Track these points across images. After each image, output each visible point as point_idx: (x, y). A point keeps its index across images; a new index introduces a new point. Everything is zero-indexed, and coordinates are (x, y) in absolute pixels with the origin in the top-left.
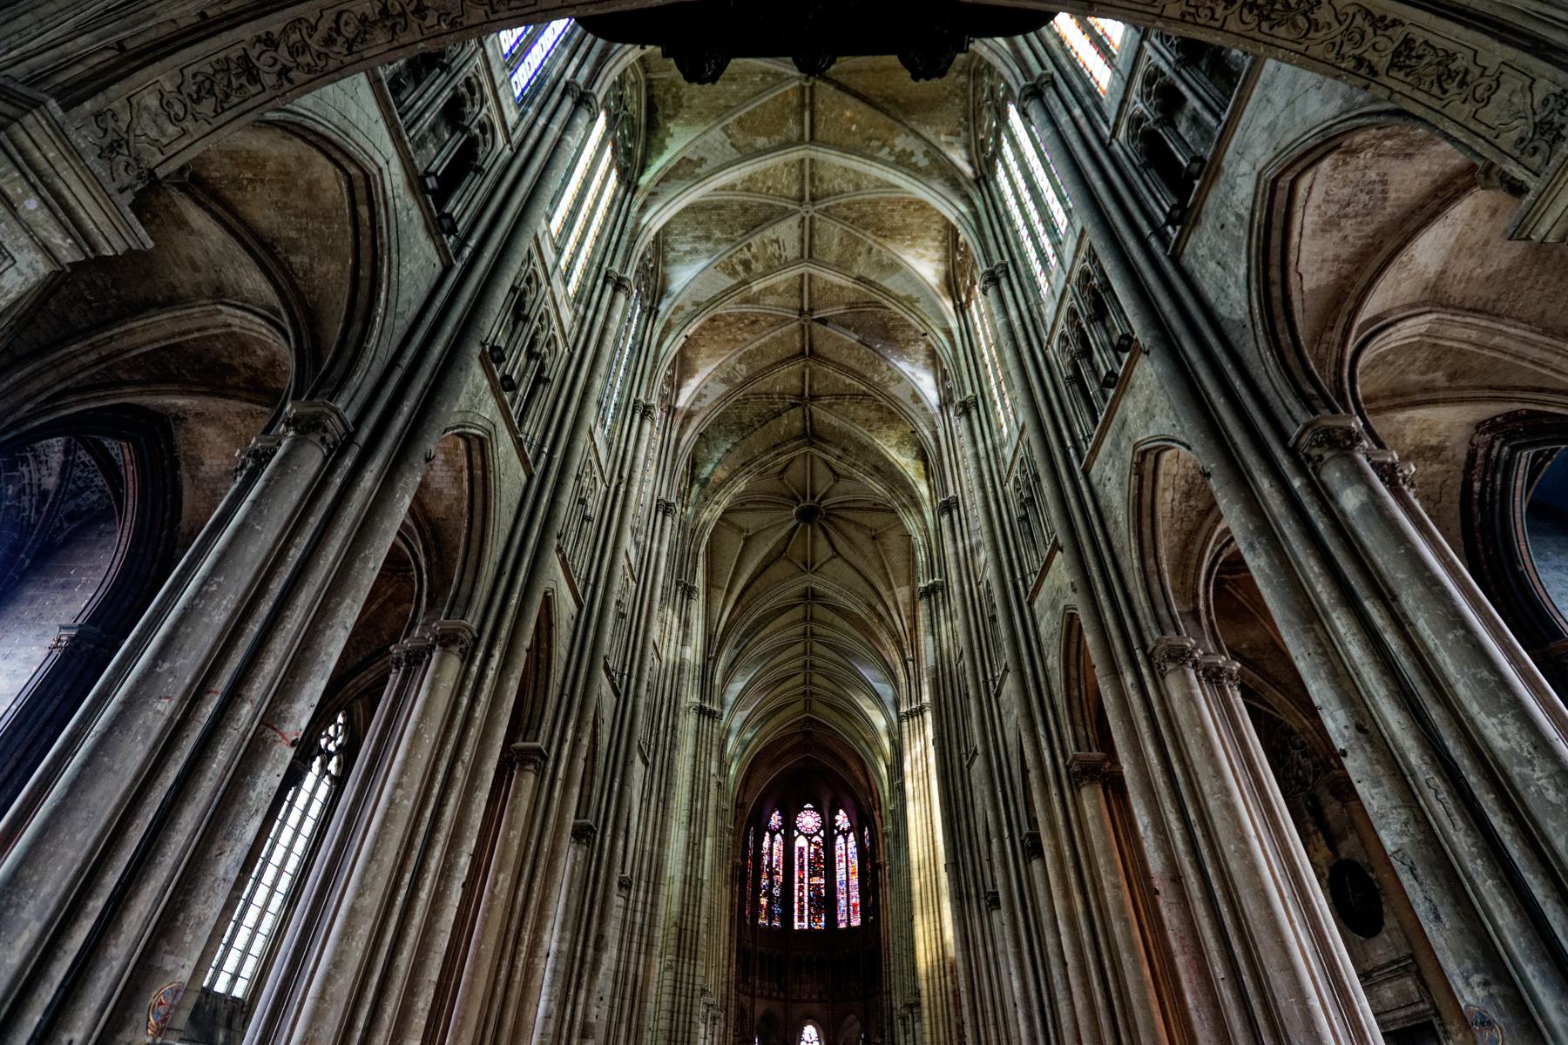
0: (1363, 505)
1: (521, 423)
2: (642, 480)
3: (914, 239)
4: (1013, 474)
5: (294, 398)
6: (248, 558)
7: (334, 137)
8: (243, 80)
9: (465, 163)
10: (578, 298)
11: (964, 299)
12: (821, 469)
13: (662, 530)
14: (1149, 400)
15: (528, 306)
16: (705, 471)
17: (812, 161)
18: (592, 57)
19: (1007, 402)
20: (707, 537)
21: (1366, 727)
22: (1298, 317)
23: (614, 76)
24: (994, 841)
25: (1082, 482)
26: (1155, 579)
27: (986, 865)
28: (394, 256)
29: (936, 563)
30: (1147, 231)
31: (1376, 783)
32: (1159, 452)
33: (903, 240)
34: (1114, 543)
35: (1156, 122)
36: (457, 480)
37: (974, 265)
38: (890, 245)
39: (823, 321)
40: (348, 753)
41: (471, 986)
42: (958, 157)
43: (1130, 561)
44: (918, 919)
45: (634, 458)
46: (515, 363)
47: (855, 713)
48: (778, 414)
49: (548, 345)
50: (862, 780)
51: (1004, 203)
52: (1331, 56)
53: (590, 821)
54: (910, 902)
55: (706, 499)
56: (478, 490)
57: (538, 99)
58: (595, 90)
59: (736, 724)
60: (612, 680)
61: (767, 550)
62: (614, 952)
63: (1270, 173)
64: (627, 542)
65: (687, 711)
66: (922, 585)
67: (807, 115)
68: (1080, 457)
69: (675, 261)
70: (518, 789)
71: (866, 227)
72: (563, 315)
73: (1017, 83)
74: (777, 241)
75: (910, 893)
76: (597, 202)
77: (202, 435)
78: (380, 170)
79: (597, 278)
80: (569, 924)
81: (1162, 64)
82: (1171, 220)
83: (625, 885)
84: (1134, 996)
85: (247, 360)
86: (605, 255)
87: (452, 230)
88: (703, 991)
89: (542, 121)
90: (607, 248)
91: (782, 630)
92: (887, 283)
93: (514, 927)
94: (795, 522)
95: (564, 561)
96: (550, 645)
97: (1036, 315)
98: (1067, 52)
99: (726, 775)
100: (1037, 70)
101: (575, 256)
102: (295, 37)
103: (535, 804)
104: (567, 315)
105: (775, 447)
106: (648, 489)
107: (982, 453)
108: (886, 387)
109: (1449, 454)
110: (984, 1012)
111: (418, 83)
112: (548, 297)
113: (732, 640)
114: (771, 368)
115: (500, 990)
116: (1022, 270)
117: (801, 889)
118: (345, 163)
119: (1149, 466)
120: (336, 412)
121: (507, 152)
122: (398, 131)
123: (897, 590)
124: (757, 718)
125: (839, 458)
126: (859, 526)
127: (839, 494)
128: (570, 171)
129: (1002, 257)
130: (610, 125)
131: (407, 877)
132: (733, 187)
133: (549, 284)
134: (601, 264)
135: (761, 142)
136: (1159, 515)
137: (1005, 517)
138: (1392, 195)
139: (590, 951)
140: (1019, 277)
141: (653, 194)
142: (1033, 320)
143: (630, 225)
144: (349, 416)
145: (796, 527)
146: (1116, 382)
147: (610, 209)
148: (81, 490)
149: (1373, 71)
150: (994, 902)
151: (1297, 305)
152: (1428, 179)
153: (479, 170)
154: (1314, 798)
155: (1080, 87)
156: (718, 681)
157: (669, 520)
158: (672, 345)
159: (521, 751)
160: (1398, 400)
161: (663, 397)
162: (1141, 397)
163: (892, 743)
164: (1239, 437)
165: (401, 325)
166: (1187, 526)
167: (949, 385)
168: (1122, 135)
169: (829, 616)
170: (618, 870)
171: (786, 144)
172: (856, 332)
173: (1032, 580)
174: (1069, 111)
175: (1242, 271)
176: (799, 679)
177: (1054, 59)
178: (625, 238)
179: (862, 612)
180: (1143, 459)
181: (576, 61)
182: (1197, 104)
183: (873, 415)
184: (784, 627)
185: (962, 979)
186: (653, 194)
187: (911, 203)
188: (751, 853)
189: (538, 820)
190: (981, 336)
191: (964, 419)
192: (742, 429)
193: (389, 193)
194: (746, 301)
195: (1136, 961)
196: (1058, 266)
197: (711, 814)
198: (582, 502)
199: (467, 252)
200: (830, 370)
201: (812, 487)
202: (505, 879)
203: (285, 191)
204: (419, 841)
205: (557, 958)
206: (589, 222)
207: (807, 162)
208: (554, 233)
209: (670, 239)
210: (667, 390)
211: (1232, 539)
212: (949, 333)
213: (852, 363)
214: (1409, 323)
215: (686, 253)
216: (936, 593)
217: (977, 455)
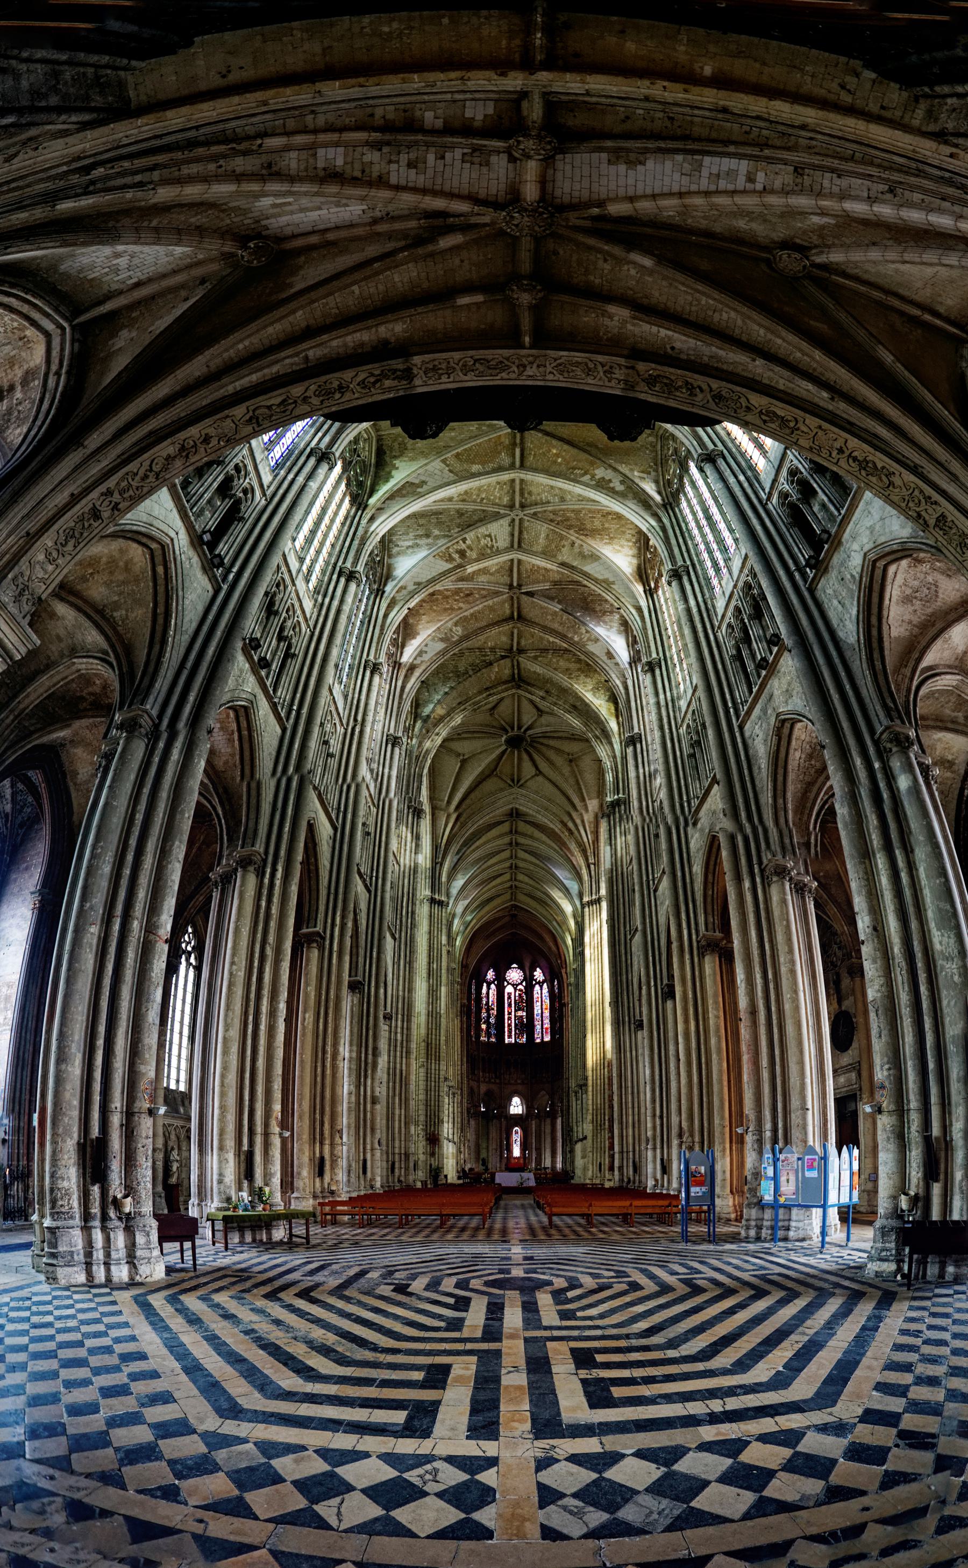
0: (909, 788)
1: (275, 691)
2: (374, 721)
3: (611, 538)
4: (686, 721)
5: (120, 709)
6: (113, 827)
7: (143, 530)
8: (92, 521)
9: (232, 516)
10: (317, 591)
11: (653, 585)
12: (526, 705)
13: (391, 758)
14: (789, 684)
15: (277, 603)
16: (427, 710)
17: (522, 481)
18: (334, 430)
19: (685, 666)
20: (429, 761)
21: (878, 929)
22: (887, 653)
23: (351, 437)
24: (644, 988)
25: (737, 734)
26: (782, 814)
27: (637, 1004)
28: (180, 593)
29: (621, 783)
30: (793, 568)
31: (874, 962)
32: (794, 722)
33: (602, 539)
34: (757, 782)
35: (798, 500)
36: (230, 741)
37: (662, 563)
38: (591, 541)
39: (530, 594)
40: (199, 949)
41: (301, 1077)
42: (650, 488)
43: (766, 798)
44: (589, 1036)
45: (366, 704)
46: (269, 648)
47: (549, 902)
48: (491, 664)
49: (294, 629)
50: (554, 948)
51: (687, 524)
52: (903, 505)
53: (360, 978)
54: (584, 1027)
55: (428, 732)
56: (246, 746)
57: (288, 463)
58: (334, 449)
59: (459, 909)
60: (364, 881)
61: (480, 769)
62: (386, 1058)
63: (872, 556)
64: (364, 771)
65: (422, 902)
66: (608, 799)
67: (518, 451)
68: (737, 716)
69: (399, 554)
70: (308, 960)
71: (569, 527)
72: (305, 605)
73: (696, 451)
74: (490, 536)
75: (584, 1021)
76: (332, 521)
77: (75, 754)
78: (172, 540)
79: (332, 574)
80: (355, 1042)
81: (800, 466)
82: (808, 565)
83: (388, 1017)
84: (715, 1076)
85: (90, 689)
86: (339, 556)
87: (221, 564)
88: (446, 1079)
89: (290, 477)
90: (341, 551)
91: (494, 840)
92: (588, 568)
93: (320, 1044)
94: (504, 747)
95: (320, 797)
96: (316, 860)
97: (710, 606)
98: (733, 441)
99: (453, 946)
100: (711, 446)
101: (314, 561)
102: (124, 484)
103: (321, 969)
104: (308, 605)
105: (487, 689)
106: (378, 727)
107: (662, 703)
108: (584, 646)
109: (955, 768)
110: (626, 1087)
111: (200, 477)
112: (293, 595)
113: (454, 848)
114: (483, 629)
115: (319, 1079)
116: (700, 572)
117: (509, 1019)
118: (149, 543)
119: (786, 731)
120: (146, 711)
121: (263, 502)
122: (186, 512)
123: (588, 802)
124: (475, 905)
125: (543, 698)
126: (559, 751)
127: (542, 726)
128: (312, 504)
129: (684, 561)
130: (345, 469)
131: (251, 1018)
132: (450, 499)
133: (294, 584)
134: (335, 564)
135: (475, 468)
136: (790, 767)
137: (678, 753)
138: (941, 596)
139: (370, 1057)
140: (697, 577)
141: (380, 509)
142: (707, 610)
143: (360, 532)
144: (154, 713)
145: (503, 753)
146: (768, 667)
147: (343, 524)
148: (22, 807)
149: (926, 524)
150: (640, 1026)
151: (886, 644)
152: (959, 594)
153: (242, 519)
154: (838, 975)
155: (743, 463)
156: (444, 879)
157: (397, 750)
158: (397, 616)
159: (306, 935)
160: (939, 724)
161: (390, 656)
162: (784, 681)
163: (577, 923)
164: (845, 725)
165: (186, 639)
166: (808, 779)
167: (638, 647)
168: (775, 500)
169: (530, 830)
170: (382, 1007)
171: (500, 469)
172: (559, 602)
173: (694, 803)
174: (736, 477)
175: (854, 612)
176: (507, 877)
177: (723, 442)
178: (356, 542)
179: (557, 828)
180: (783, 726)
181: (320, 434)
182: (825, 499)
183: (573, 666)
184: (494, 838)
185: (614, 1070)
186: (380, 509)
187: (609, 513)
188: (473, 996)
189: (325, 979)
190: (666, 615)
191: (649, 675)
192: (458, 676)
193: (177, 552)
194: (462, 579)
195: (720, 1059)
196: (728, 575)
197: (444, 971)
198: (326, 743)
199: (231, 576)
200: (536, 631)
201: (519, 720)
202: (310, 1017)
203: (111, 573)
204: (253, 996)
205: (350, 1061)
206: (326, 536)
207: (517, 482)
208: (298, 547)
209: (394, 539)
210: (393, 650)
211: (833, 795)
212: (639, 609)
213: (556, 626)
214: (948, 677)
215: (408, 547)
216: (619, 806)
217: (658, 703)
